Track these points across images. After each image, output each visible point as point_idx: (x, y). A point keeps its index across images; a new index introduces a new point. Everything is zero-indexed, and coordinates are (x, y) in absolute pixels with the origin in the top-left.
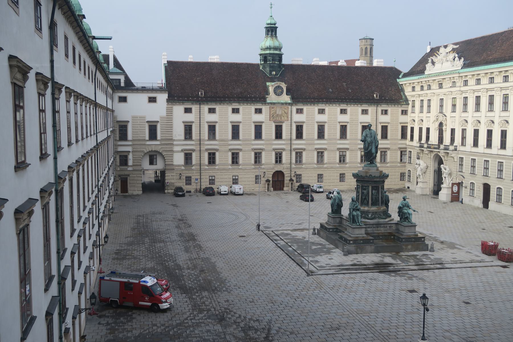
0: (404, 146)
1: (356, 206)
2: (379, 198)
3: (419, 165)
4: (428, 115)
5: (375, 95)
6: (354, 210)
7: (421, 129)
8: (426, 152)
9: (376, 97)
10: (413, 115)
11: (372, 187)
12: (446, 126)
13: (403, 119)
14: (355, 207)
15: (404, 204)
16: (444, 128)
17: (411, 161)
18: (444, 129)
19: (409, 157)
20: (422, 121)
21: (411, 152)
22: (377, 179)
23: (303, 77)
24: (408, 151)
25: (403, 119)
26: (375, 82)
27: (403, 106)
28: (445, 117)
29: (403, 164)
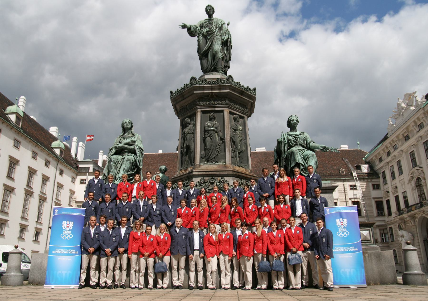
0: (384, 223)
1: (128, 141)
2: (223, 139)
3: (403, 236)
4: (402, 177)
5: (341, 172)
6: (120, 151)
7: (397, 198)
8: (408, 219)
9: (342, 173)
10: (386, 186)
11: (203, 112)
12: (425, 179)
13: (375, 193)
14: (127, 144)
15: (290, 138)
16: (423, 181)
17: (393, 239)
18: (422, 184)
19: (391, 235)
20: (396, 187)
21: (391, 228)
22: (212, 88)
23: (264, 161)
24: (388, 229)
25: (375, 193)
26: (339, 161)
27: (373, 180)
28: (421, 169)
29: (385, 245)
